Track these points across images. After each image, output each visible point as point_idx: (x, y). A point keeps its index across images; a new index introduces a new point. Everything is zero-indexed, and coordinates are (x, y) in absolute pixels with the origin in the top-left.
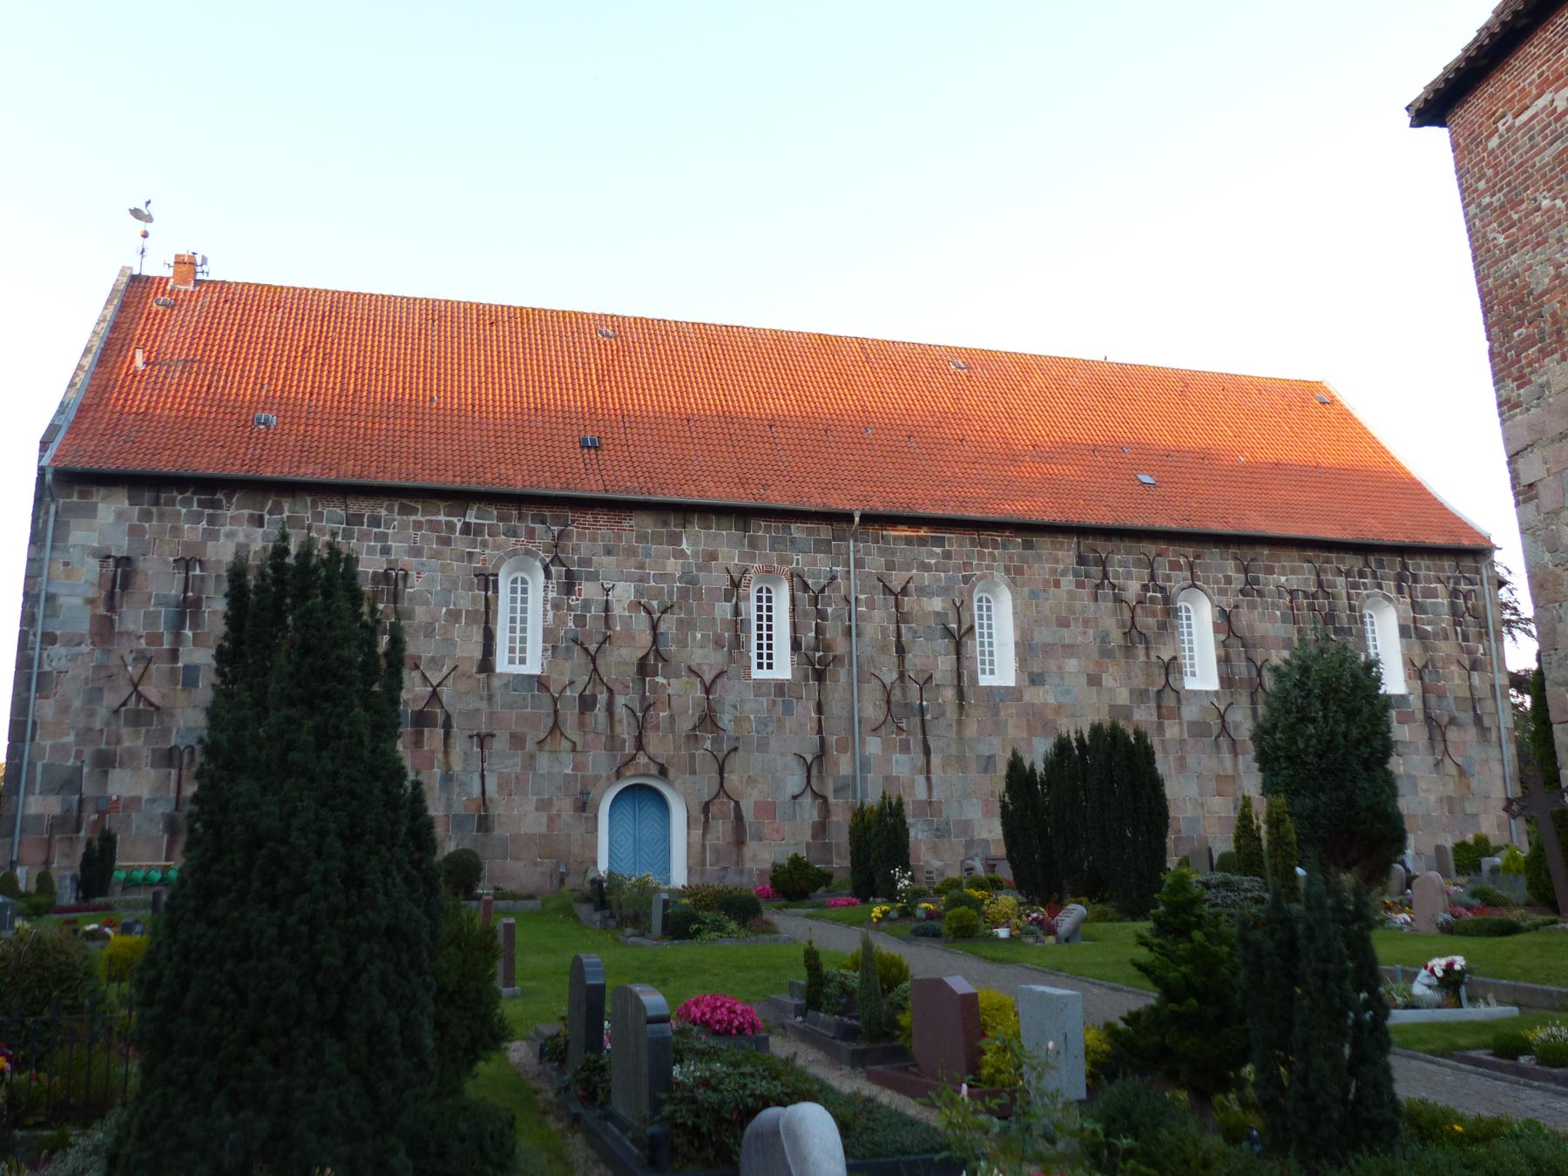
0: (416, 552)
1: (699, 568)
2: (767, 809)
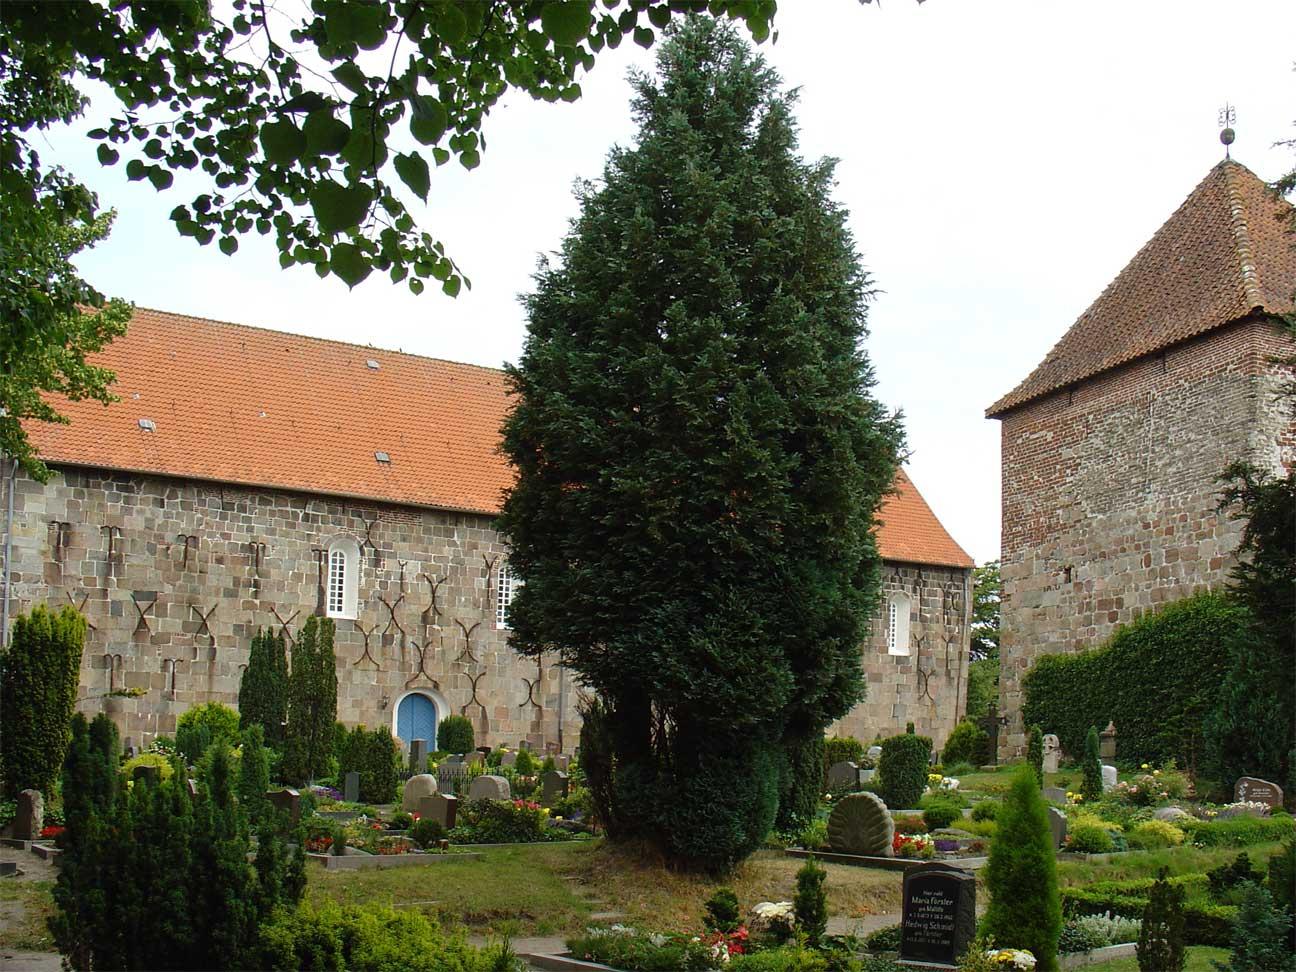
0: (272, 532)
1: (465, 554)
2: (503, 712)
